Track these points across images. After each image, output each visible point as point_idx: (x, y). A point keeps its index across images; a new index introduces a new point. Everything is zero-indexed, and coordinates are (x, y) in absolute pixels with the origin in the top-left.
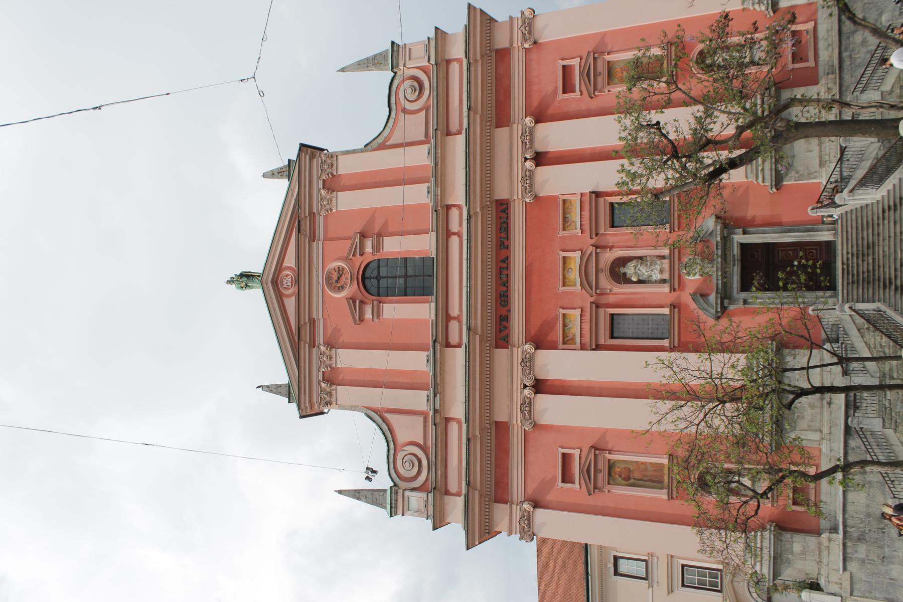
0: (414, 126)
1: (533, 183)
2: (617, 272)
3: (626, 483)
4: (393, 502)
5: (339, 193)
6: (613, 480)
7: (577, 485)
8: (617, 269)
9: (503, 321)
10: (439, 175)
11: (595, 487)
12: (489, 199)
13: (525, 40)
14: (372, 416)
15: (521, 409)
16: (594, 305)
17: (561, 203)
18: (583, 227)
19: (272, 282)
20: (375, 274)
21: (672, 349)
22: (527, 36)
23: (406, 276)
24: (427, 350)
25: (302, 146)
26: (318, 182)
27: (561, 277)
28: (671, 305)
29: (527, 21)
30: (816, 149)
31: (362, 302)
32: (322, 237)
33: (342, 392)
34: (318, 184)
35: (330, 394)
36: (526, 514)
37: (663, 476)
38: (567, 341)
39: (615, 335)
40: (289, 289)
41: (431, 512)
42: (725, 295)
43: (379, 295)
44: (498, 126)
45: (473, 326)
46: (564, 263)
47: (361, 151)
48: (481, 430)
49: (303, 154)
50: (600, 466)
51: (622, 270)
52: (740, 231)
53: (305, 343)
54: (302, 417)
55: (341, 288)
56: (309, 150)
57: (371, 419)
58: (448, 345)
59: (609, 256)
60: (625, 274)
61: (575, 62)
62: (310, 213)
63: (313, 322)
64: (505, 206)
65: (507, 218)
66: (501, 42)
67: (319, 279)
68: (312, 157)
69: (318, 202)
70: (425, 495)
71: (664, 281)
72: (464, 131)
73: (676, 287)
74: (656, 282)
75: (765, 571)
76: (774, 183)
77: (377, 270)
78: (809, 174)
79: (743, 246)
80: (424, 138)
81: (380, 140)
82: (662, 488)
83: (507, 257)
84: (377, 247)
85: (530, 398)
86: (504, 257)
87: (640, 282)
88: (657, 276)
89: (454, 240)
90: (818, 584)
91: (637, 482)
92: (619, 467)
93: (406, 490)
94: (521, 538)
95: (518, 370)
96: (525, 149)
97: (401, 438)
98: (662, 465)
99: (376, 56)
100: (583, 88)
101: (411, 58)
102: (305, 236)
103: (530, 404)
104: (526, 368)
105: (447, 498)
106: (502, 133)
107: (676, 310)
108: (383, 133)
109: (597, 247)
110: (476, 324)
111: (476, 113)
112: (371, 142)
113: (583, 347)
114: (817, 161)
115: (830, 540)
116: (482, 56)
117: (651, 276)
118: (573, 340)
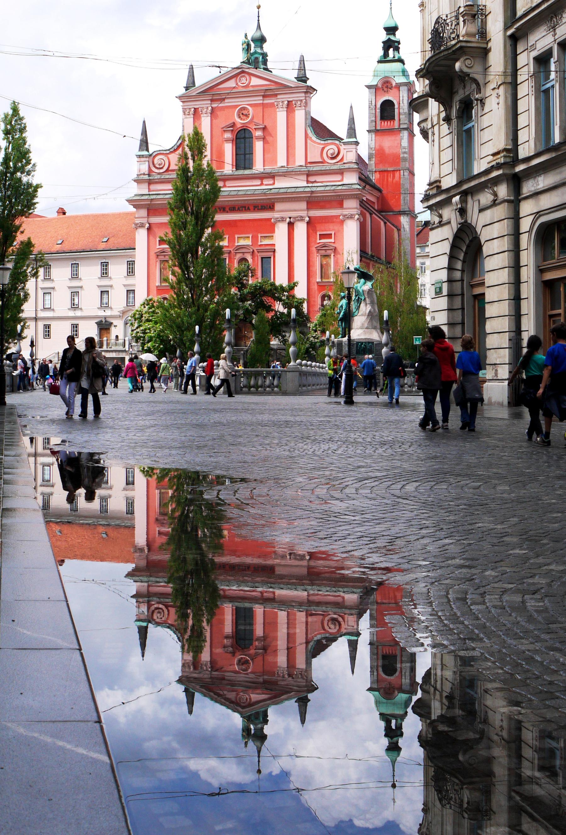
0: (314, 156)
7: (158, 247)
11: (158, 255)
13: (344, 216)
31: (232, 130)
32: (265, 102)
33: (190, 120)
34: (291, 97)
35: (189, 115)
43: (236, 139)
44: (308, 203)
55: (240, 117)
61: (332, 240)
63: (224, 99)
67: (243, 102)
68: (306, 93)
80: (308, 161)
82: (161, 283)
84: (258, 138)
89: (258, 182)
96: (295, 218)
97: (169, 156)
100: (321, 244)
101: (348, 153)
105: (147, 184)
106: (304, 205)
111: (311, 194)
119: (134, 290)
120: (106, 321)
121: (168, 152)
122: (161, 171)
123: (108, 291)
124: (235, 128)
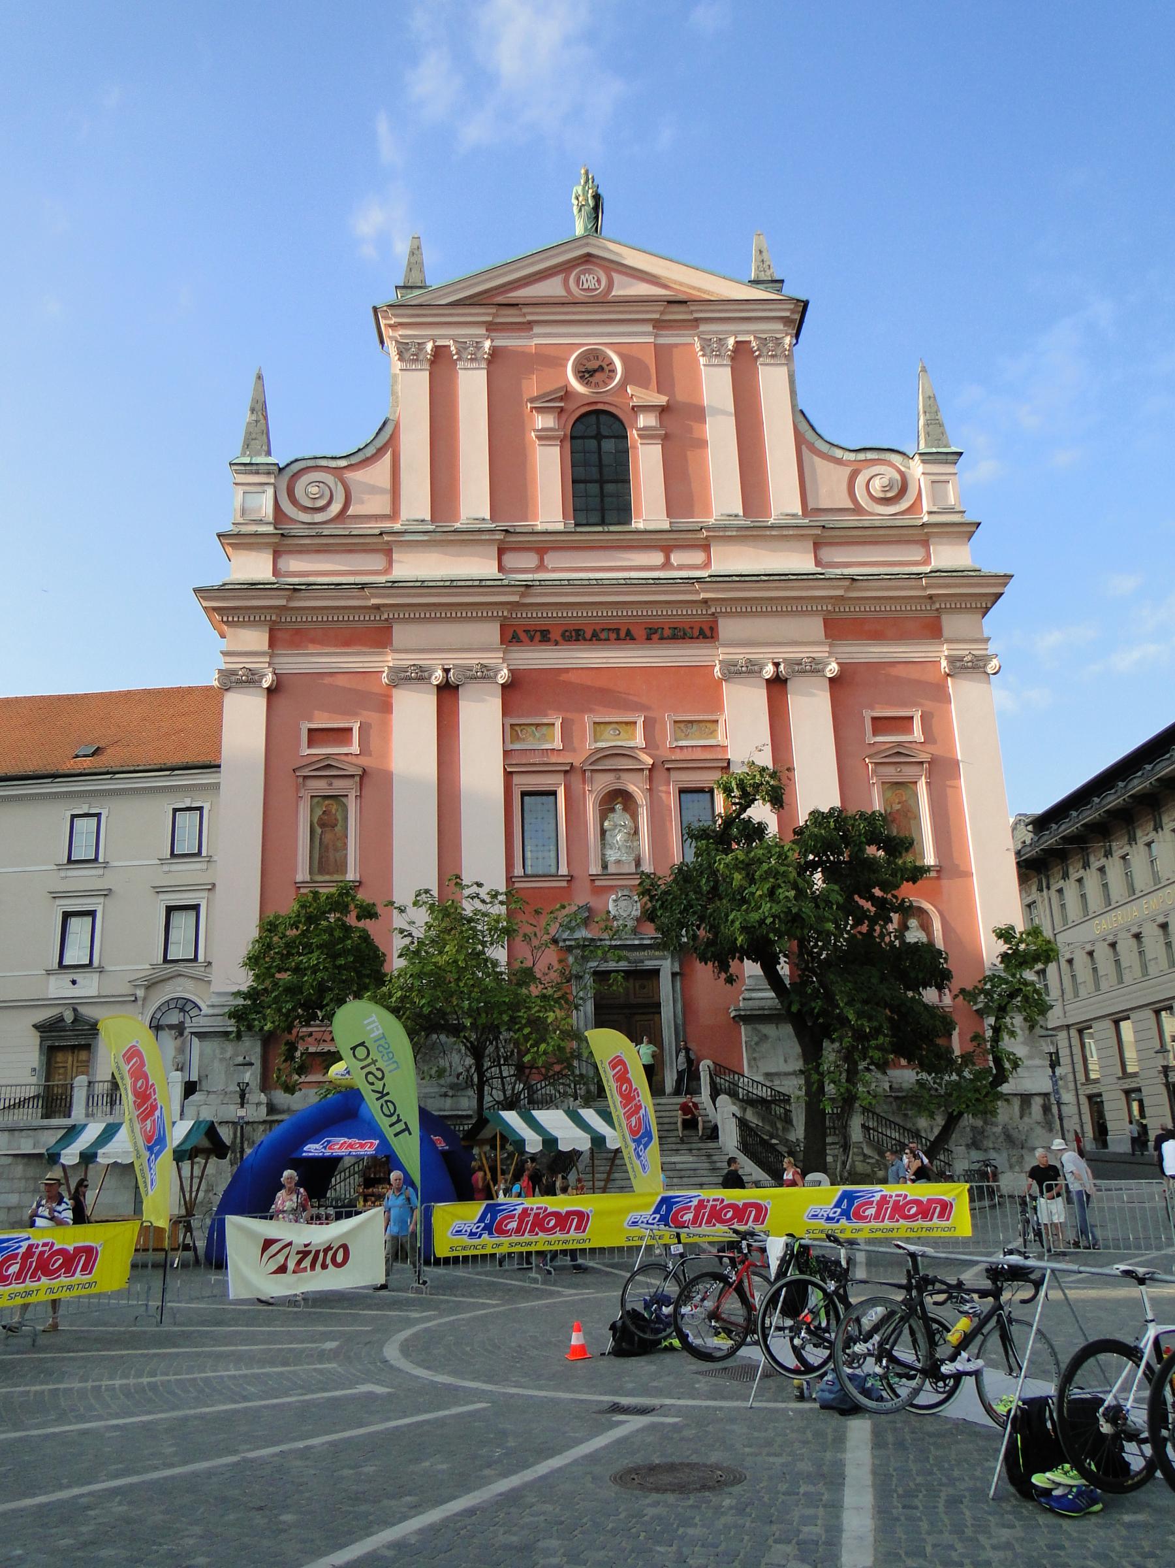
1: (742, 675)
2: (618, 798)
3: (315, 820)
4: (254, 468)
5: (729, 369)
6: (318, 802)
8: (620, 799)
9: (542, 636)
10: (755, 533)
11: (305, 777)
12: (718, 610)
14: (385, 429)
15: (414, 665)
16: (568, 768)
17: (714, 718)
18: (678, 750)
19: (589, 255)
20: (605, 432)
21: (510, 879)
22: (958, 664)
23: (602, 482)
24: (493, 519)
25: (806, 304)
26: (748, 332)
27: (607, 720)
28: (572, 876)
29: (981, 664)
30: (791, 1070)
31: (562, 410)
32: (661, 341)
36: (256, 677)
37: (328, 873)
38: (512, 731)
39: (527, 798)
40: (578, 286)
41: (245, 529)
42: (588, 947)
43: (572, 438)
44: (827, 623)
45: (533, 590)
46: (627, 723)
47: (794, 406)
48: (377, 607)
49: (792, 306)
50: (338, 783)
51: (619, 807)
52: (678, 970)
53: (495, 315)
54: (375, 309)
56: (797, 317)
57: (380, 430)
58: (501, 552)
59: (636, 788)
60: (613, 810)
61: (917, 734)
62: (696, 320)
63: (530, 325)
64: (708, 633)
65: (692, 638)
66: (952, 624)
68: (786, 321)
69: (715, 333)
70: (271, 518)
71: (605, 866)
72: (819, 570)
73: (598, 883)
74: (603, 855)
75: (203, 1021)
76: (743, 1013)
77: (611, 434)
78: (755, 1059)
79: (656, 973)
80: (811, 505)
81: (810, 435)
82: (310, 873)
83: (633, 639)
84: (647, 435)
85: (430, 678)
86: (635, 632)
87: (603, 832)
88: (612, 856)
89: (657, 558)
90: (193, 1093)
91: (318, 837)
92: (337, 810)
93: (275, 487)
94: (220, 671)
95: (472, 660)
96: (790, 663)
97: (352, 476)
98: (345, 872)
99: (941, 425)
101: (936, 484)
102: (662, 313)
103: (420, 679)
104: (474, 672)
106: (814, 627)
107: (564, 884)
108: (820, 441)
109: (650, 770)
110: (536, 595)
111: (847, 589)
112: (808, 421)
113: (506, 753)
114: (773, 1071)
115: (258, 1104)
116: (930, 597)
117: (611, 848)
118: (516, 738)
119: (196, 908)
120: (75, 1021)
121: (343, 463)
122: (319, 517)
123: (92, 914)
124: (571, 406)
